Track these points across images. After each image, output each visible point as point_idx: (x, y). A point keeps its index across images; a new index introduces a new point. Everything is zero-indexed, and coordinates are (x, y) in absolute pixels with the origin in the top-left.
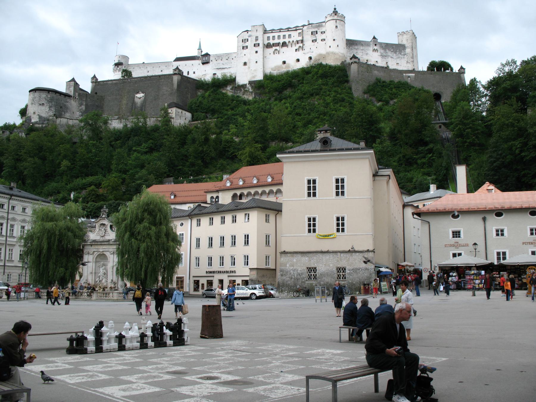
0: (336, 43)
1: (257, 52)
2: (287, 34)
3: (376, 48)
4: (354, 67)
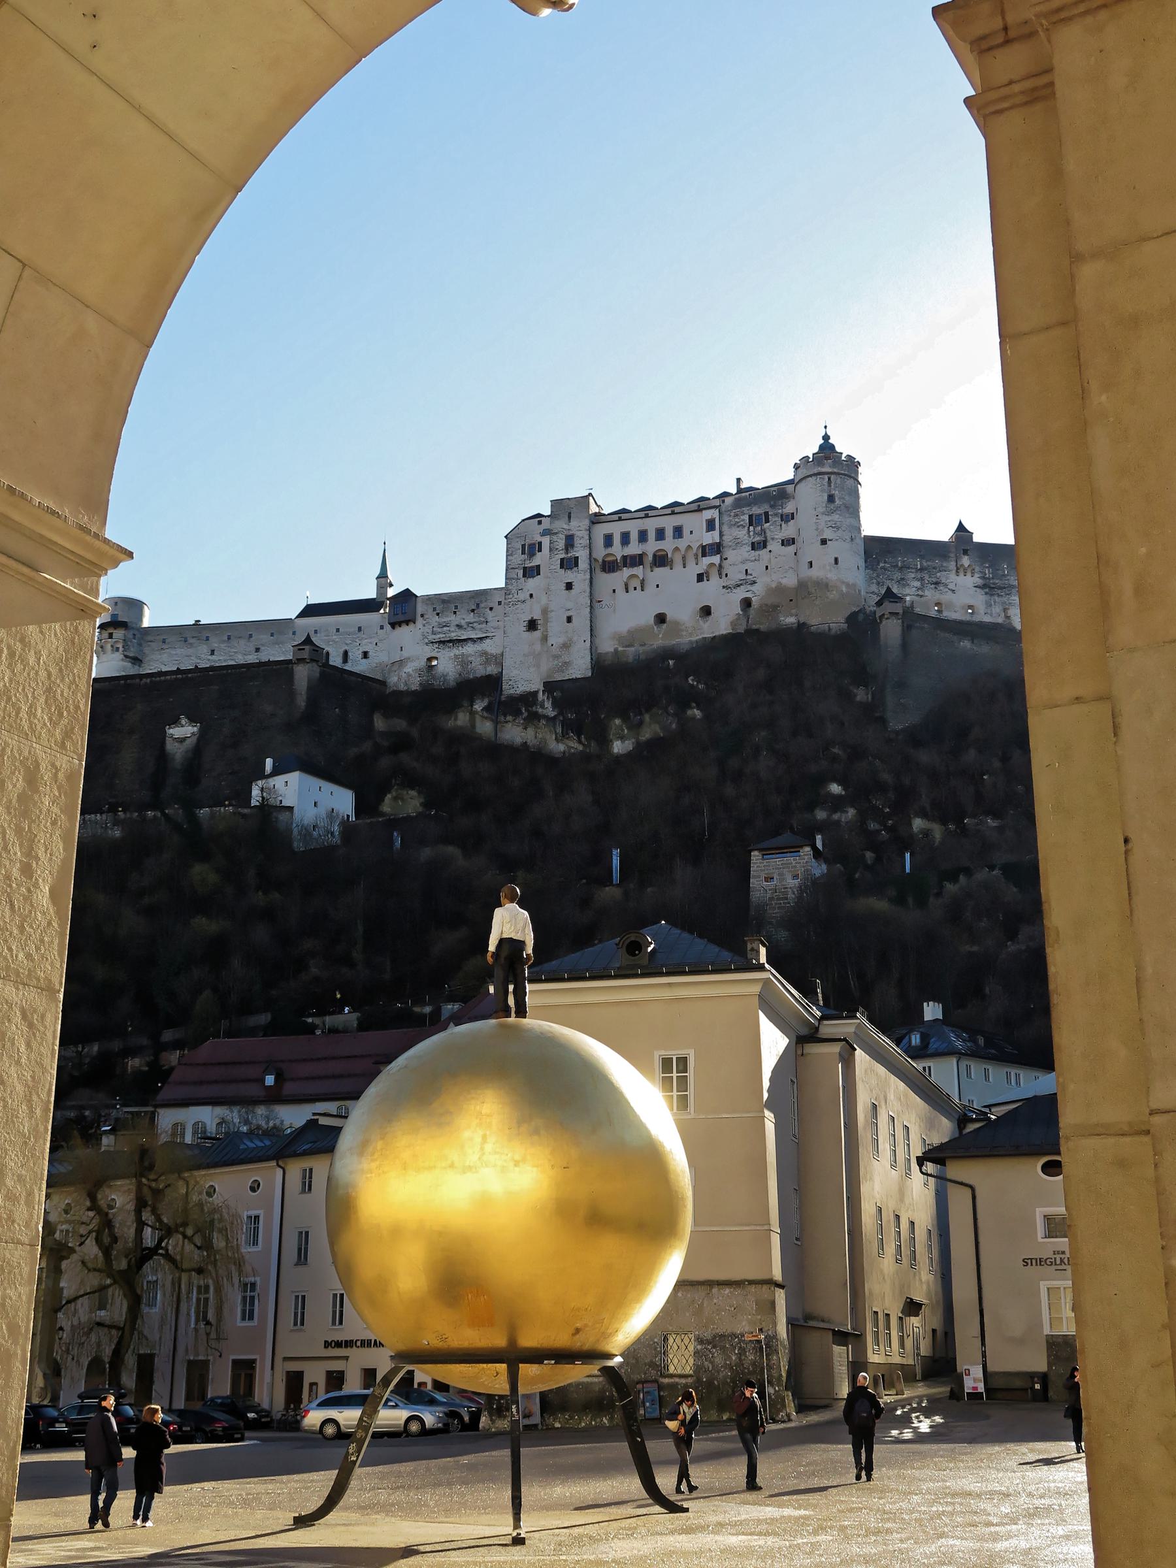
0: (833, 549)
1: (569, 586)
2: (669, 523)
4: (891, 630)
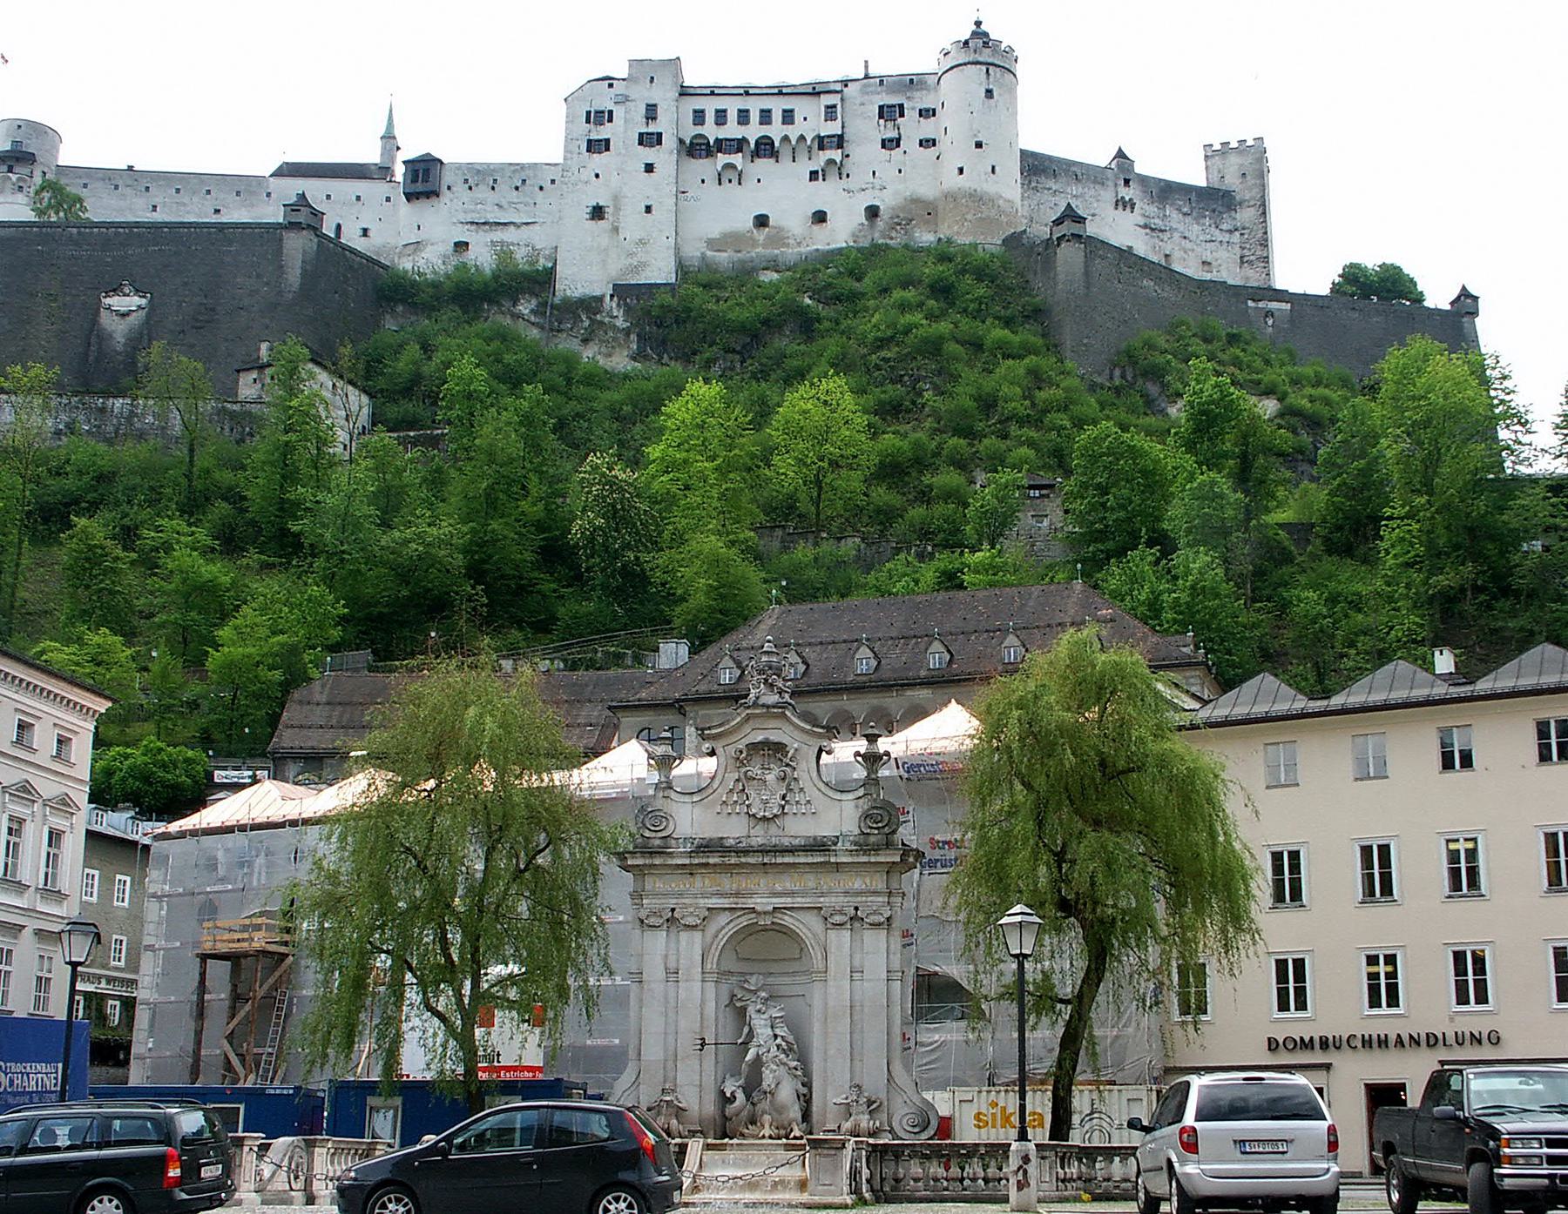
1: (649, 168)
2: (777, 106)
3: (1127, 193)
4: (1069, 257)
